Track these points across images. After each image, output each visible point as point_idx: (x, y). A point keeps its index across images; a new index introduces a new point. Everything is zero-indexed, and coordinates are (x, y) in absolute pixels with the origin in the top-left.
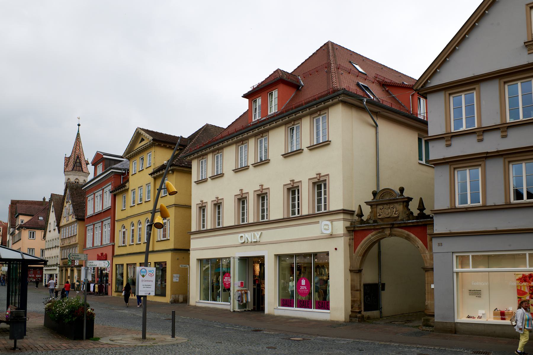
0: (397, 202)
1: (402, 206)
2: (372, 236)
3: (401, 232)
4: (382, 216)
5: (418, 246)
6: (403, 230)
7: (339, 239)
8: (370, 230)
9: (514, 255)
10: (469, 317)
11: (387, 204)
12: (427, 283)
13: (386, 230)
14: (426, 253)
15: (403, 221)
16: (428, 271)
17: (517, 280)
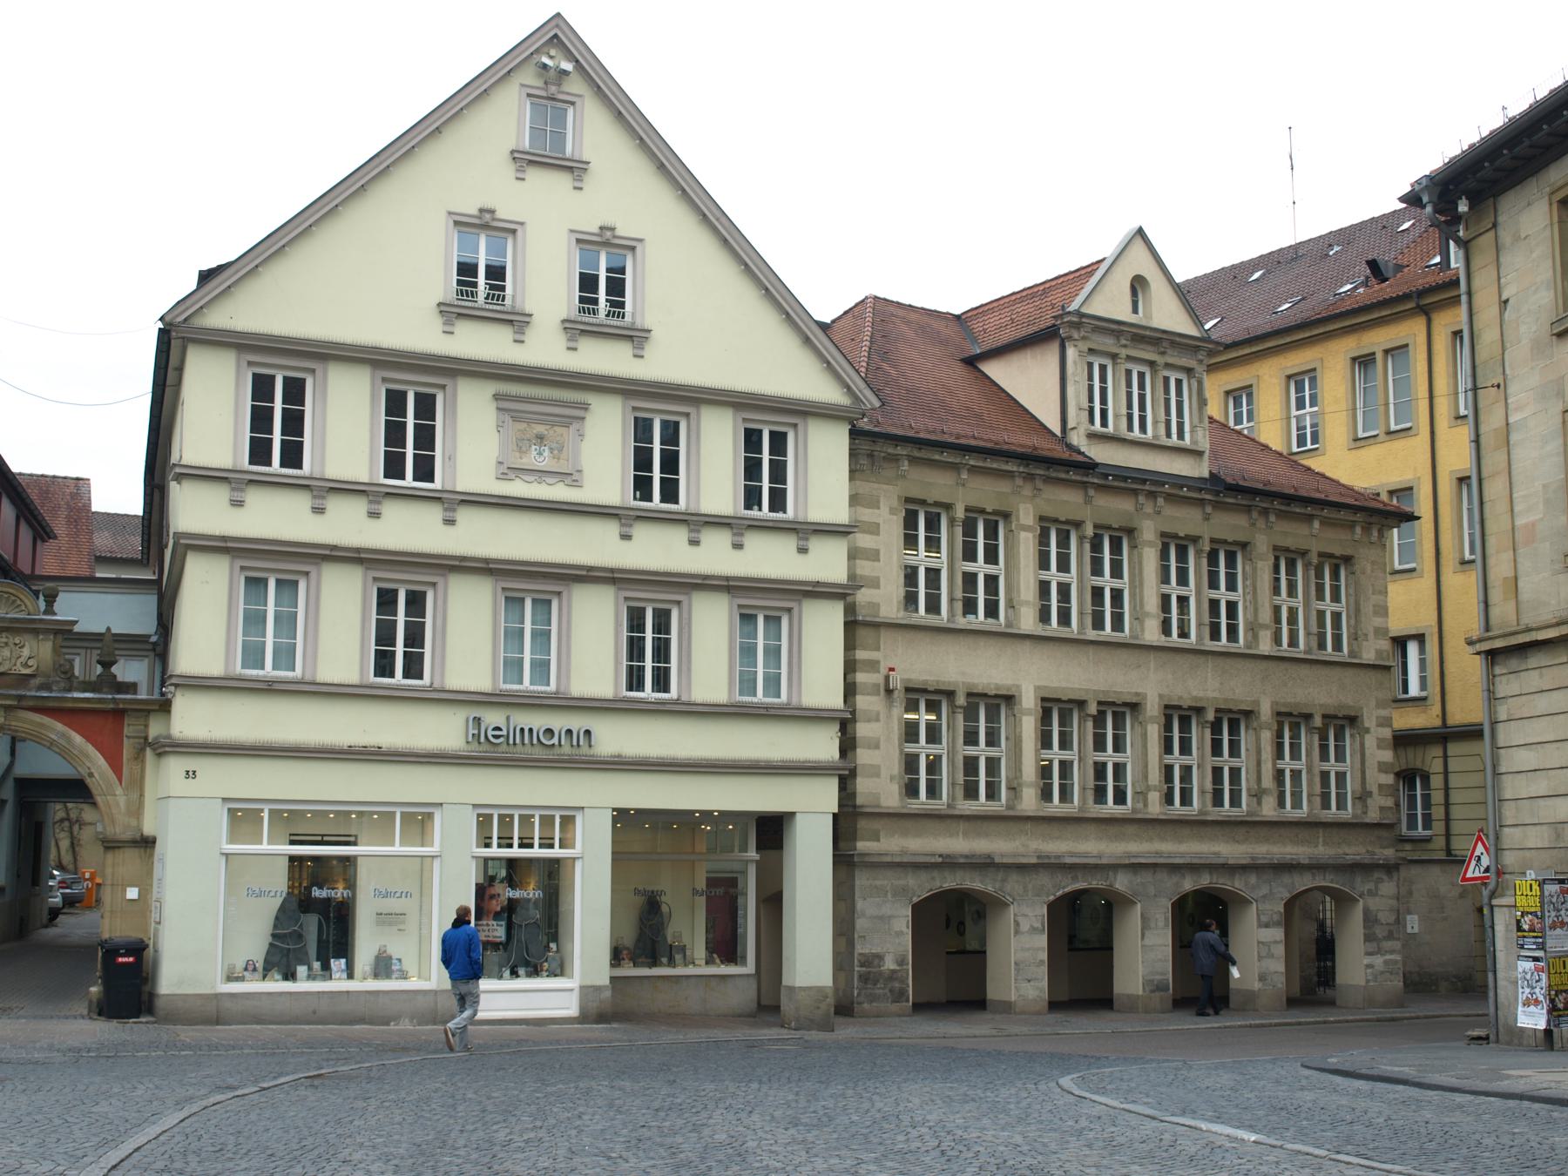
5: (93, 771)
6: (46, 720)
12: (112, 885)
14: (117, 793)
16: (119, 847)
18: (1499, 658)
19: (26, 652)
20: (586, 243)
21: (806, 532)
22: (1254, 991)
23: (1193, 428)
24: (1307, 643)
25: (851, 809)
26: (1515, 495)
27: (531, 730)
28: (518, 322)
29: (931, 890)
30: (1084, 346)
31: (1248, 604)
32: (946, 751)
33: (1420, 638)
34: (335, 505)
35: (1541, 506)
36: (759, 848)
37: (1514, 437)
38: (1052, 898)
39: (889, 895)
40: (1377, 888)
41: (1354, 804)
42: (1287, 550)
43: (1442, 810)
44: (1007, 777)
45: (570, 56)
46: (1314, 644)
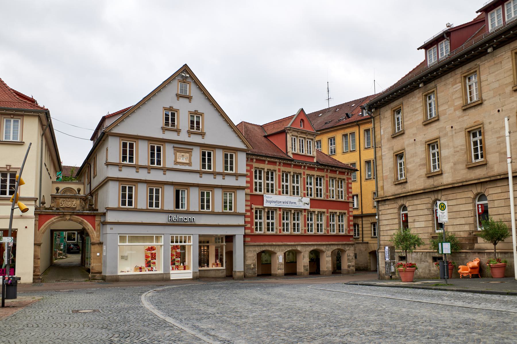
0: (76, 198)
1: (79, 201)
2: (55, 219)
3: (78, 218)
4: (63, 206)
7: (33, 219)
8: (53, 215)
9: (144, 236)
10: (122, 272)
11: (68, 198)
13: (67, 216)
15: (79, 211)
17: (146, 250)
18: (380, 202)
19: (74, 203)
20: (192, 114)
21: (237, 176)
23: (313, 152)
24: (336, 197)
26: (383, 169)
27: (182, 218)
28: (178, 131)
30: (291, 134)
33: (357, 196)
34: (141, 170)
35: (389, 172)
36: (226, 242)
37: (383, 158)
41: (345, 231)
42: (332, 177)
43: (361, 232)
45: (188, 74)
46: (337, 198)
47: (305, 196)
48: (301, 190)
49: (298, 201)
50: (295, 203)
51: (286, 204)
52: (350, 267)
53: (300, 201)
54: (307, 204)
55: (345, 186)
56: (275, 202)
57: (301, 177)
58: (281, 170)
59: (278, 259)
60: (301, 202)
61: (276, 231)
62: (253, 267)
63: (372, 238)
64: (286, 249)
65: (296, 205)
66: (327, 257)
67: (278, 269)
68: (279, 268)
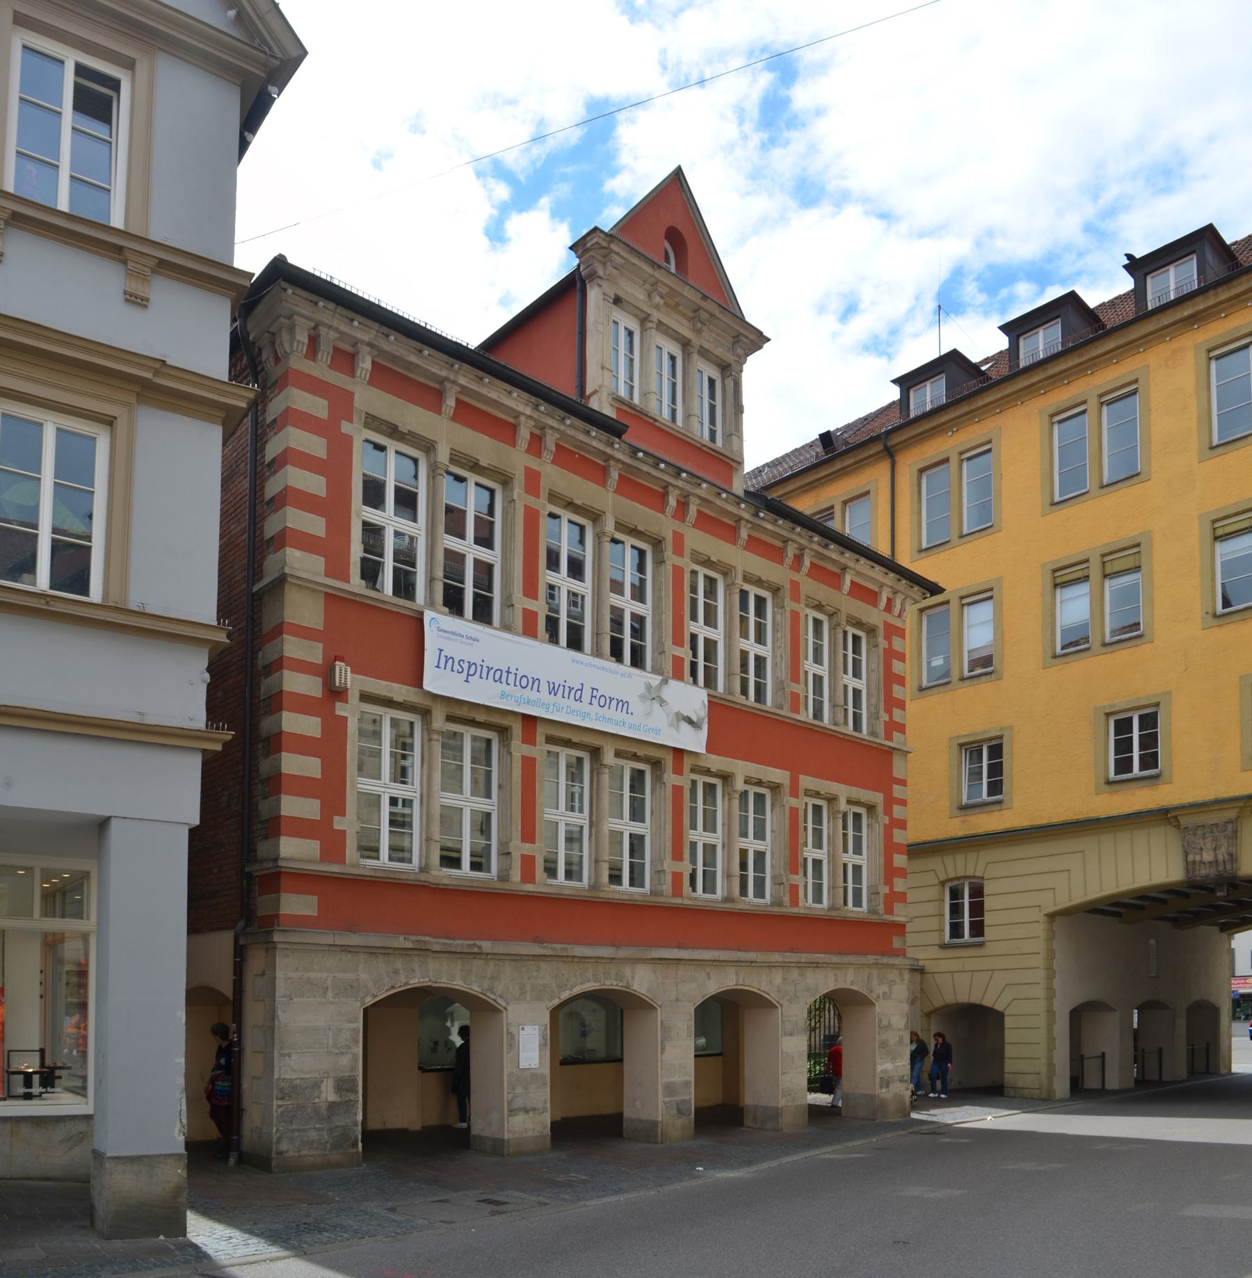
22: (778, 1108)
25: (271, 865)
29: (393, 987)
31: (778, 659)
32: (418, 795)
38: (556, 1002)
39: (330, 994)
40: (890, 992)
41: (869, 901)
44: (499, 839)
47: (678, 676)
48: (658, 641)
49: (642, 697)
50: (623, 704)
51: (571, 702)
52: (888, 1086)
53: (654, 696)
54: (689, 721)
55: (873, 666)
56: (499, 675)
57: (659, 562)
58: (545, 485)
59: (511, 1046)
60: (656, 705)
61: (499, 871)
62: (332, 1097)
63: (944, 947)
64: (562, 987)
65: (628, 718)
66: (785, 1034)
67: (513, 1112)
68: (519, 1103)
